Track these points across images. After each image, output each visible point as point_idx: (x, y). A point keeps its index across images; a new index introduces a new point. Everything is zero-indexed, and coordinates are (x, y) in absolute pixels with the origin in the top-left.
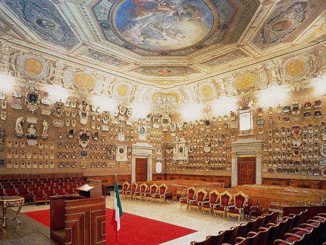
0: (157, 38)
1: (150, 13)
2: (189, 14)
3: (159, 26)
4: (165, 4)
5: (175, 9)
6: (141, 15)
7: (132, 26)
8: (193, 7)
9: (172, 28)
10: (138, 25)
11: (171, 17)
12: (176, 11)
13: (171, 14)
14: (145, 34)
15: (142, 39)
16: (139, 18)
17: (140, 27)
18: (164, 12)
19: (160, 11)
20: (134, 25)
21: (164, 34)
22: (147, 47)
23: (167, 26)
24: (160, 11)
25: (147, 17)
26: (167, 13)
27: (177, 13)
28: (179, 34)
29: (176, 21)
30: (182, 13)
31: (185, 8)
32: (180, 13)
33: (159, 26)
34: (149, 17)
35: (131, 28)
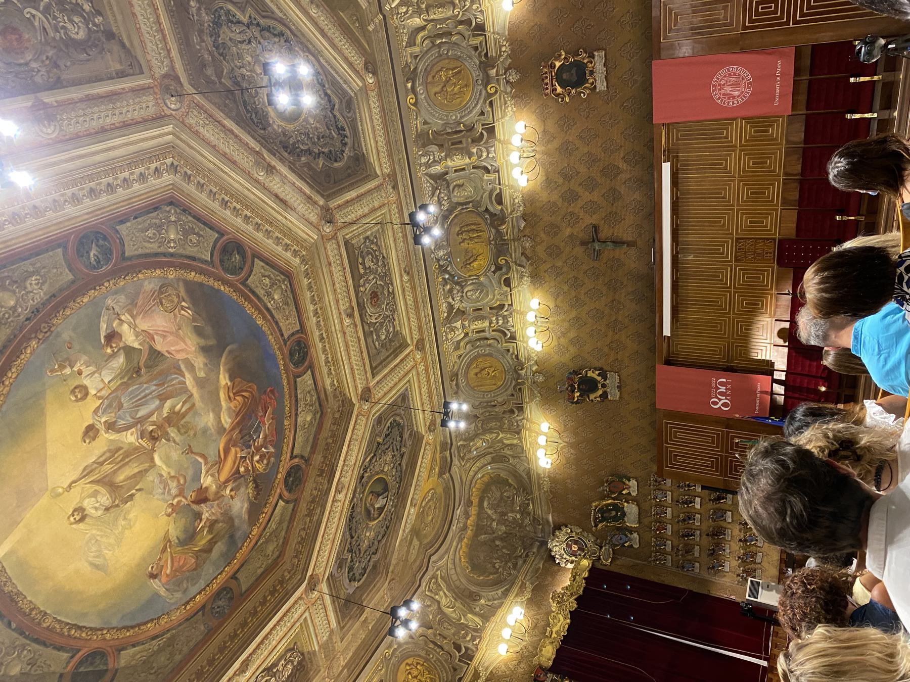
0: (112, 402)
1: (229, 421)
2: (189, 537)
3: (172, 432)
4: (242, 469)
5: (218, 496)
6: (234, 392)
7: (202, 342)
8: (208, 550)
9: (151, 477)
10: (199, 361)
11: (197, 477)
12: (211, 497)
13: (207, 481)
14: (148, 365)
15: (130, 338)
16: (224, 380)
17: (191, 368)
18: (220, 462)
19: (227, 451)
20: (205, 350)
21: (130, 438)
22: (65, 327)
23: (167, 460)
24: (227, 451)
25: (220, 406)
26: (214, 470)
27: (204, 500)
28: (105, 499)
29: (174, 491)
30: (198, 516)
31: (212, 524)
32: (204, 508)
33: (172, 432)
34: (217, 415)
35: (199, 331)
